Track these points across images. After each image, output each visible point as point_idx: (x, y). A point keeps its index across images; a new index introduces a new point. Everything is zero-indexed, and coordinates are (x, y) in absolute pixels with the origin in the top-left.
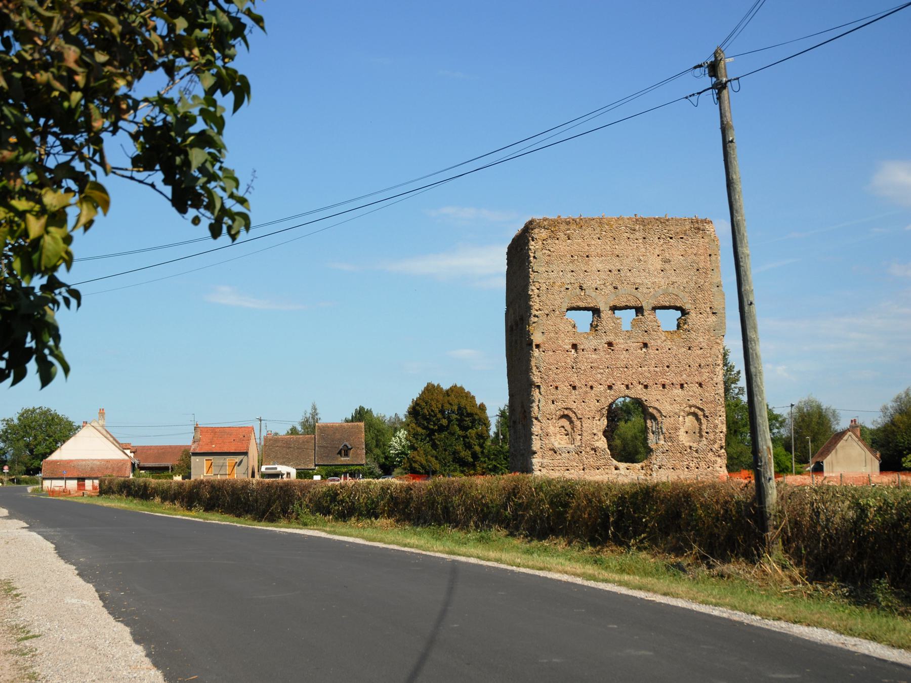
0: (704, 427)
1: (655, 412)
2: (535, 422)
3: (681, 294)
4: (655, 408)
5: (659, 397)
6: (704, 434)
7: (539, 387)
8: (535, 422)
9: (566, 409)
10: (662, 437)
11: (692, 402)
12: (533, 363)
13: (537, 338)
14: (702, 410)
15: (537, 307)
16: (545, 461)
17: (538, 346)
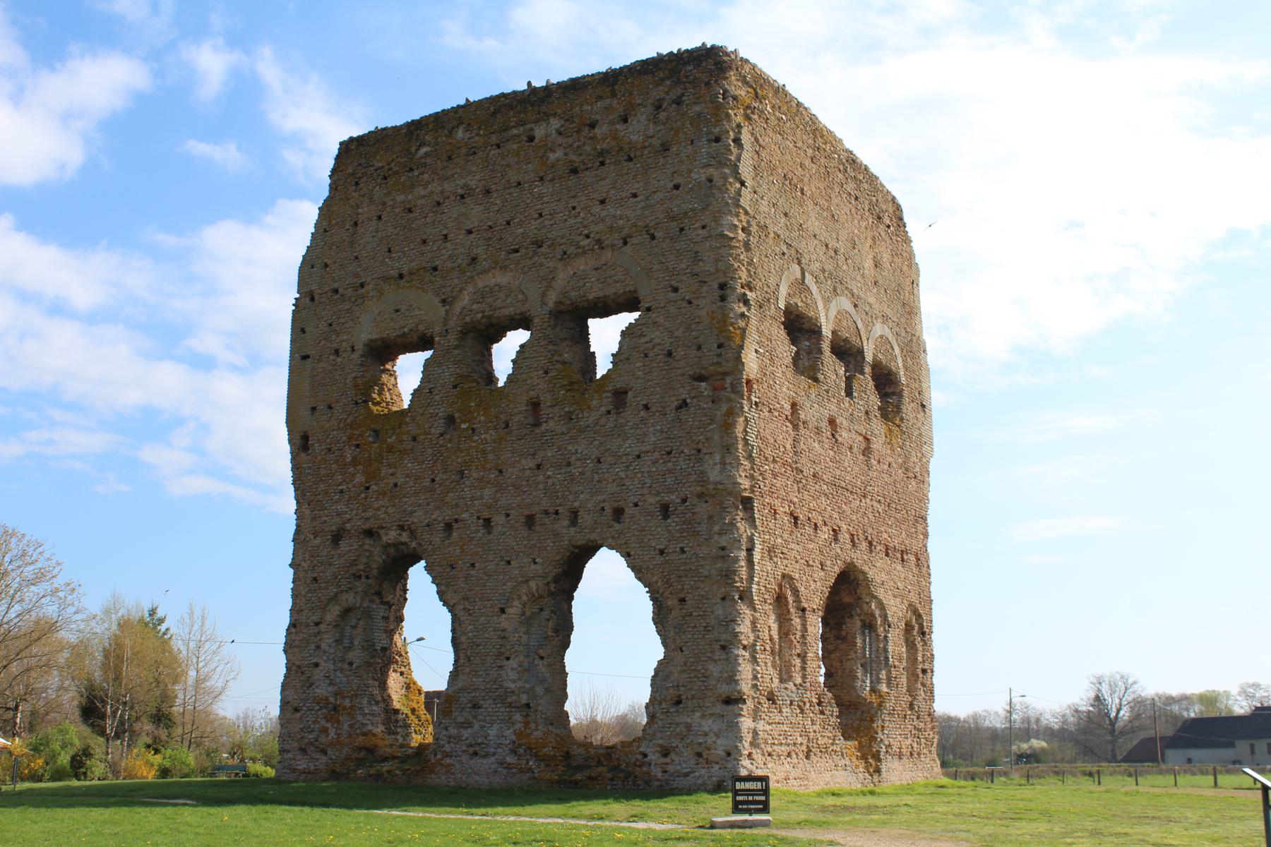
0: (920, 659)
1: (877, 613)
2: (743, 608)
3: (897, 350)
4: (882, 606)
5: (884, 576)
6: (919, 672)
7: (747, 503)
8: (743, 608)
9: (784, 576)
10: (883, 675)
11: (915, 599)
12: (739, 428)
13: (751, 363)
14: (919, 616)
15: (743, 274)
16: (761, 726)
17: (748, 382)
